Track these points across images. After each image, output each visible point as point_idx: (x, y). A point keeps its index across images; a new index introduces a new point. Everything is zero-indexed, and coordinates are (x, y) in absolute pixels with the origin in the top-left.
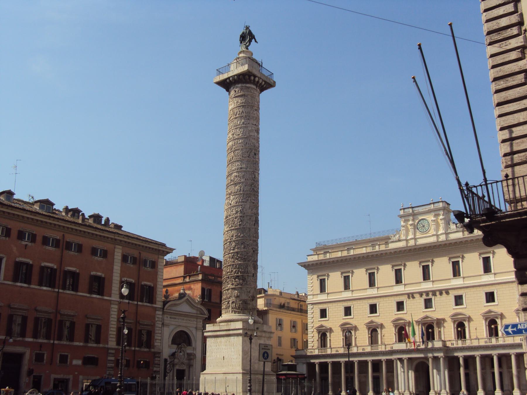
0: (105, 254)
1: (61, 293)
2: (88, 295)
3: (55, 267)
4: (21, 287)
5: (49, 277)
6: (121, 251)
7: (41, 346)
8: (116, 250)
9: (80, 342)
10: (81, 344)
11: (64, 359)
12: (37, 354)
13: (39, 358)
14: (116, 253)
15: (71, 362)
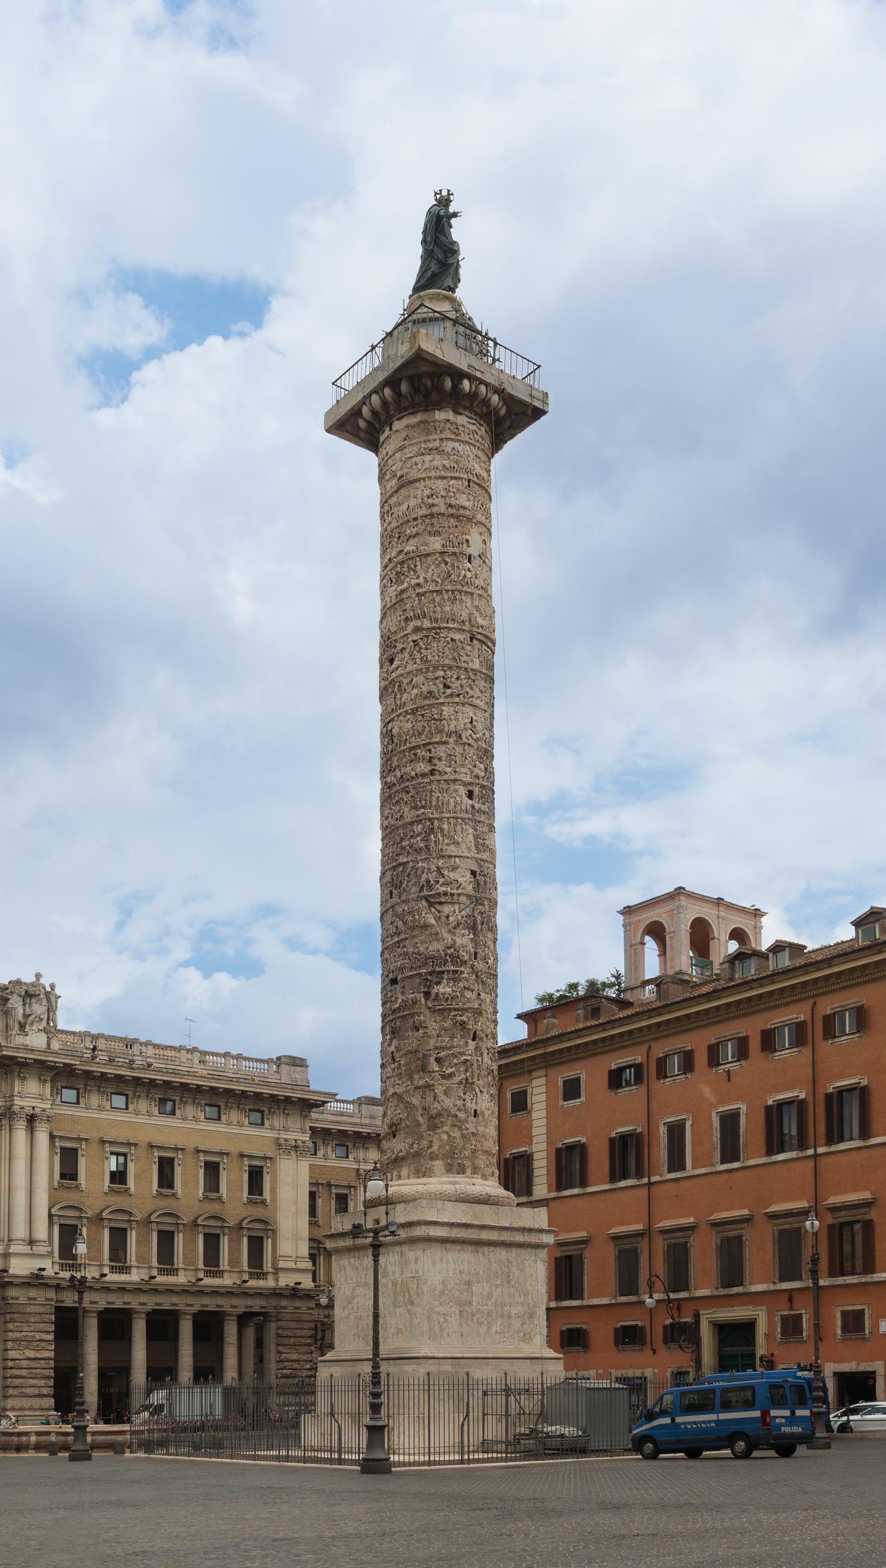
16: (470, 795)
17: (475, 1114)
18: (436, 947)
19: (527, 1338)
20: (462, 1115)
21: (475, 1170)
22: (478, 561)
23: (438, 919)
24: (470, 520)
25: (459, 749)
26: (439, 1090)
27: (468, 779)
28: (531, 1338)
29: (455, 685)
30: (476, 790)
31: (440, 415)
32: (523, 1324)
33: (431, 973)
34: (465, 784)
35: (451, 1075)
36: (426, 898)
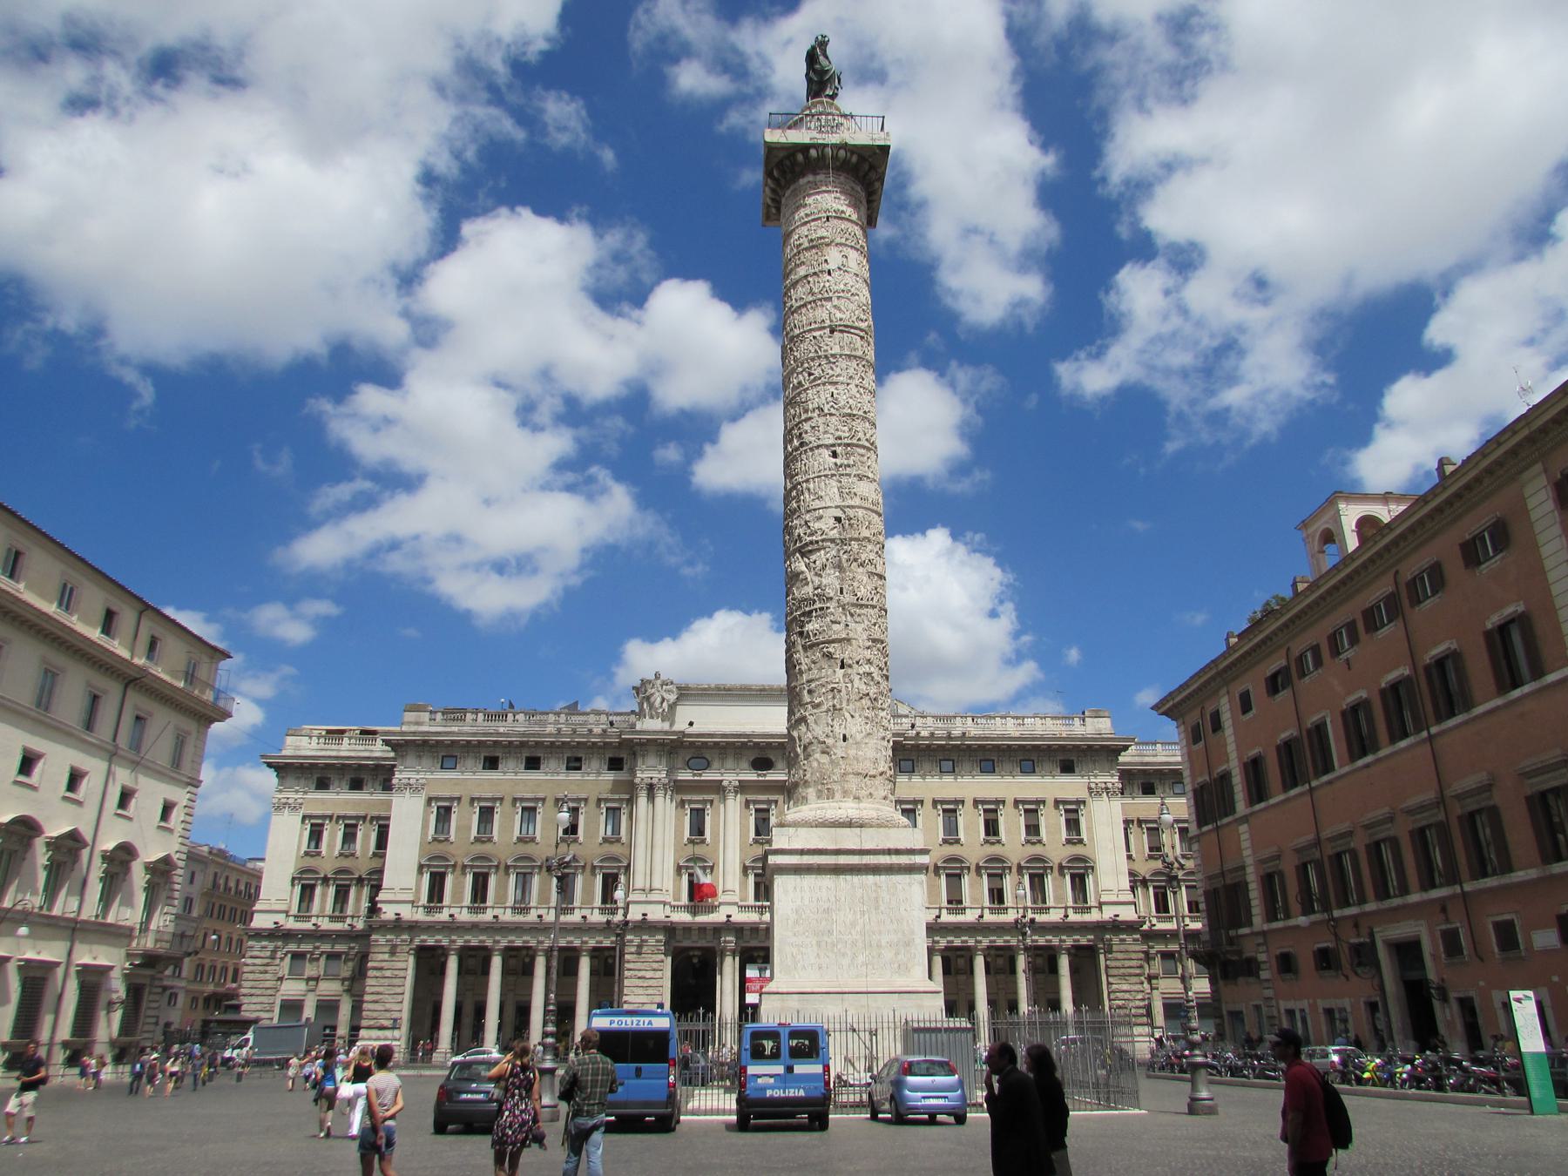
0: (1501, 534)
2: (1499, 702)
3: (1407, 672)
4: (1367, 766)
6: (1543, 480)
7: (1444, 910)
8: (1527, 492)
9: (1531, 866)
10: (1533, 873)
11: (1506, 934)
13: (1451, 943)
15: (1529, 941)
16: (835, 455)
17: (845, 739)
18: (809, 590)
19: (903, 968)
20: (830, 741)
21: (845, 793)
22: (836, 274)
23: (807, 566)
25: (821, 420)
26: (811, 719)
27: (831, 441)
28: (908, 970)
29: (817, 372)
30: (839, 450)
31: (802, 181)
32: (897, 954)
33: (803, 614)
34: (827, 447)
35: (818, 706)
36: (799, 550)
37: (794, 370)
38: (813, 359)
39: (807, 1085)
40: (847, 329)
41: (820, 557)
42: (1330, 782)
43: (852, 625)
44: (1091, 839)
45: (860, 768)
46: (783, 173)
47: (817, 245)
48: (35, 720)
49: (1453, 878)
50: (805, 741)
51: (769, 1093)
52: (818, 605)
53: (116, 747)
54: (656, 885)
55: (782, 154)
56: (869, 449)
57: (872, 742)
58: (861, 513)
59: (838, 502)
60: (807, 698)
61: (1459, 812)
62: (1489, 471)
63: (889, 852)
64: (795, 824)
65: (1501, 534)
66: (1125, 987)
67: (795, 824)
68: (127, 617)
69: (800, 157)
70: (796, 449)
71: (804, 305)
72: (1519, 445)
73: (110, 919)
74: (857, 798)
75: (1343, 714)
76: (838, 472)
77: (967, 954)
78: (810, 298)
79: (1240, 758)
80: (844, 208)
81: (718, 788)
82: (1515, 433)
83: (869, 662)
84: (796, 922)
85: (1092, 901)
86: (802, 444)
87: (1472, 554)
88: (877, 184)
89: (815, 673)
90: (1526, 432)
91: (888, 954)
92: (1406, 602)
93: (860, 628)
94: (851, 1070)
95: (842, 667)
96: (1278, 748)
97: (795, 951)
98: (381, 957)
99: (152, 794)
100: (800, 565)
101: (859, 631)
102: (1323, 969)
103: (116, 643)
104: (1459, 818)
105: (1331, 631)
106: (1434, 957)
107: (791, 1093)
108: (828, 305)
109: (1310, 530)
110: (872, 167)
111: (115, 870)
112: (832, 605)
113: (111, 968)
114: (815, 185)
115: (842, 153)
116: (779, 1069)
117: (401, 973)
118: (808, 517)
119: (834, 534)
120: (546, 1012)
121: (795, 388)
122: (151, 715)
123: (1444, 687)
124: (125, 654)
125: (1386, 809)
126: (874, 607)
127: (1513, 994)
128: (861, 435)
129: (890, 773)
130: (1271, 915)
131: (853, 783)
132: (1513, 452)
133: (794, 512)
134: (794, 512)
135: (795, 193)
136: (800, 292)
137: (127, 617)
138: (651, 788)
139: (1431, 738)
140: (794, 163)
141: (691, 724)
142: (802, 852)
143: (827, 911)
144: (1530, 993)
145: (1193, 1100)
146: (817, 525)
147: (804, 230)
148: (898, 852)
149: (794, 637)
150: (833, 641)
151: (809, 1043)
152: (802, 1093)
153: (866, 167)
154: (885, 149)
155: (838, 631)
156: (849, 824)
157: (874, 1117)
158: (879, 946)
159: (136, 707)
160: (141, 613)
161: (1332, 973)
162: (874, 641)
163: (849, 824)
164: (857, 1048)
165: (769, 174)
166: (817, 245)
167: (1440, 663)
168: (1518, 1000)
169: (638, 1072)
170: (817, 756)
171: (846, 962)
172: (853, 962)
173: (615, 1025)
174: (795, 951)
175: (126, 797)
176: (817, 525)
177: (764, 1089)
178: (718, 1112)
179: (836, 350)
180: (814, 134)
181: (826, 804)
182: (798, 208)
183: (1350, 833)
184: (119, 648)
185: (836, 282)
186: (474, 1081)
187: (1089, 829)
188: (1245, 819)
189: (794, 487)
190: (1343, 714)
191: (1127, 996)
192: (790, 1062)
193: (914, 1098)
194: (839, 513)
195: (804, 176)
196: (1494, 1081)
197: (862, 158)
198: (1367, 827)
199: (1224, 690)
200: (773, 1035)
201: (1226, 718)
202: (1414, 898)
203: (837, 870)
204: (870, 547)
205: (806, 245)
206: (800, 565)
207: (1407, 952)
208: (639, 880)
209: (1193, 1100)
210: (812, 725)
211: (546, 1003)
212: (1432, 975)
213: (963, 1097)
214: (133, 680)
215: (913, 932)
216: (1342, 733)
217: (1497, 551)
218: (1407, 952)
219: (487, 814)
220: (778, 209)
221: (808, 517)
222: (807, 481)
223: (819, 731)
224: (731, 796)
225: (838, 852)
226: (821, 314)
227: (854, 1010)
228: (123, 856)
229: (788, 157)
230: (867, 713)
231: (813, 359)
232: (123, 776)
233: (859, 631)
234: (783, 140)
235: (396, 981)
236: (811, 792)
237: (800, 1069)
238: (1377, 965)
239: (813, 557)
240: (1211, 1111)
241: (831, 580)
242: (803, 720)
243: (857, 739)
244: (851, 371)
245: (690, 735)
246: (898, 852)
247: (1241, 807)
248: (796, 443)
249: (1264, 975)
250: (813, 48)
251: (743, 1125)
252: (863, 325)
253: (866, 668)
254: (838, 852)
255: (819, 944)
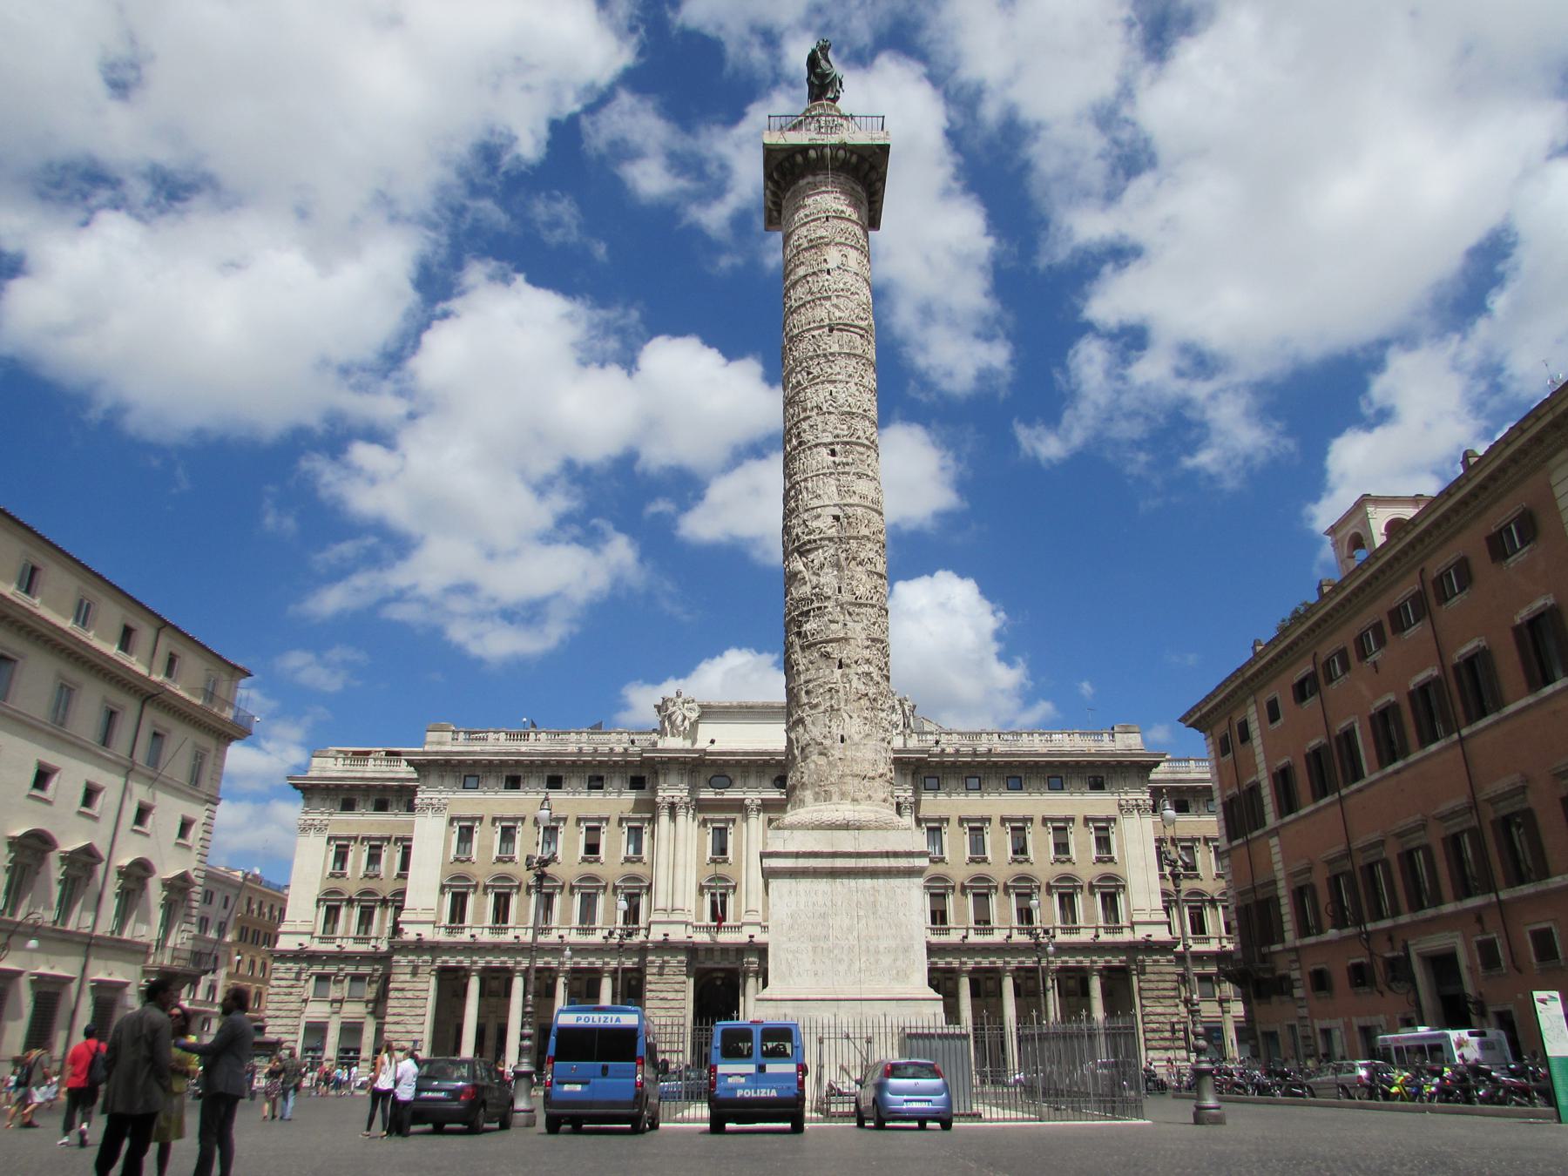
0: (1528, 525)
1: (1471, 736)
2: (1531, 699)
3: (1435, 673)
4: (1397, 772)
5: (1430, 710)
7: (1479, 920)
12: (1481, 945)
13: (1488, 954)
14: (1558, 491)
16: (833, 453)
17: (843, 740)
18: (807, 589)
19: (902, 975)
20: (827, 742)
21: (843, 795)
22: (835, 273)
24: (827, 244)
25: (820, 419)
26: (808, 721)
27: (830, 439)
28: (907, 976)
30: (838, 448)
31: (802, 182)
32: (895, 960)
33: (801, 614)
34: (825, 445)
35: (816, 706)
36: (797, 550)
37: (792, 370)
38: (811, 358)
39: (779, 1085)
40: (845, 327)
41: (818, 556)
42: (1360, 790)
43: (850, 624)
44: (1123, 857)
45: (857, 769)
46: (783, 175)
47: (816, 245)
48: (49, 734)
49: (1490, 887)
50: (803, 743)
51: (739, 1093)
52: (816, 605)
53: (134, 763)
54: (678, 905)
55: (780, 156)
56: (868, 448)
57: (871, 743)
58: (859, 511)
59: (837, 500)
60: (804, 699)
61: (1492, 816)
62: (1513, 460)
63: (887, 855)
64: (792, 827)
65: (1528, 525)
66: (1159, 1010)
67: (792, 827)
68: (145, 634)
69: (799, 158)
70: (795, 448)
71: (803, 305)
72: (1543, 431)
73: (126, 935)
74: (854, 800)
75: (1372, 718)
76: (838, 470)
77: (995, 975)
78: (809, 298)
79: (1268, 768)
80: (844, 208)
81: (740, 807)
82: (1538, 419)
83: (868, 661)
84: (791, 927)
85: (1123, 921)
86: (800, 444)
87: (1498, 547)
88: (879, 184)
89: (812, 674)
90: (1549, 417)
91: (886, 961)
92: (1432, 601)
93: (858, 627)
94: (846, 1078)
95: (840, 667)
96: (1307, 756)
97: (790, 957)
98: (402, 977)
99: (169, 810)
100: (798, 564)
101: (857, 630)
102: (1358, 985)
103: (133, 659)
104: (1493, 822)
105: (1357, 633)
106: (1471, 969)
107: (763, 1093)
108: (827, 304)
109: (1339, 535)
110: (873, 167)
111: (131, 886)
112: (830, 604)
113: (126, 984)
114: (815, 186)
115: (841, 153)
116: (751, 1068)
117: (423, 994)
118: (805, 516)
119: (832, 532)
120: (525, 1014)
121: (794, 387)
122: (168, 731)
123: (1475, 686)
124: (142, 669)
125: (1419, 816)
126: (873, 606)
127: (1537, 994)
128: (860, 433)
129: (889, 775)
130: (1304, 930)
131: (851, 785)
132: (1538, 439)
133: (792, 511)
134: (792, 511)
135: (795, 196)
136: (800, 292)
137: (145, 634)
138: (673, 808)
139: (1462, 739)
140: (794, 165)
141: (713, 742)
142: (797, 855)
143: (824, 916)
144: (1556, 994)
145: (1199, 1108)
146: (815, 524)
147: (803, 231)
148: (896, 855)
149: (793, 638)
150: (831, 641)
151: (780, 1039)
152: (774, 1093)
153: (866, 166)
154: (885, 149)
155: (836, 630)
156: (846, 826)
157: (861, 1125)
158: (877, 952)
159: (154, 724)
160: (159, 630)
161: (1367, 989)
162: (873, 640)
163: (846, 826)
164: (852, 1057)
165: (768, 176)
166: (816, 245)
167: (1470, 661)
168: (1543, 1001)
169: (605, 1070)
170: (815, 757)
171: (842, 968)
172: (848, 968)
173: (581, 1022)
174: (790, 957)
175: (142, 814)
176: (815, 524)
177: (734, 1088)
178: (695, 1120)
179: (835, 348)
180: (813, 135)
181: (823, 806)
182: (797, 210)
183: (1382, 843)
184: (136, 664)
185: (833, 282)
186: (435, 1079)
187: (1120, 847)
188: (1275, 832)
189: (793, 487)
190: (1372, 718)
191: (1161, 1019)
192: (762, 1060)
193: (896, 1102)
194: (837, 512)
195: (803, 176)
196: (1524, 1092)
197: (862, 159)
198: (1399, 835)
199: (1252, 699)
200: (745, 1034)
201: (1254, 728)
202: (1448, 908)
203: (833, 874)
204: (869, 545)
205: (806, 245)
206: (798, 564)
207: (1443, 964)
208: (661, 900)
209: (1199, 1108)
210: (810, 726)
211: (525, 1006)
212: (1469, 988)
213: (949, 1102)
214: (150, 696)
215: (912, 938)
216: (1371, 739)
217: (1524, 543)
218: (1443, 964)
219: (508, 835)
220: (780, 212)
221: (805, 516)
222: (805, 480)
223: (816, 732)
224: (753, 815)
225: (834, 855)
226: (820, 313)
227: (846, 1016)
228: (139, 872)
229: (787, 159)
230: (866, 714)
231: (811, 358)
232: (140, 792)
233: (857, 630)
234: (782, 142)
235: (417, 1002)
236: (808, 795)
237: (773, 1068)
238: (1412, 979)
239: (811, 557)
240: (1218, 1120)
241: (829, 579)
242: (801, 721)
243: (860, 743)
244: (851, 370)
245: (712, 754)
246: (896, 855)
247: (1271, 819)
248: (794, 442)
249: (1298, 993)
250: (814, 52)
251: (717, 1126)
252: (863, 324)
253: (865, 668)
254: (834, 855)
255: (814, 949)
